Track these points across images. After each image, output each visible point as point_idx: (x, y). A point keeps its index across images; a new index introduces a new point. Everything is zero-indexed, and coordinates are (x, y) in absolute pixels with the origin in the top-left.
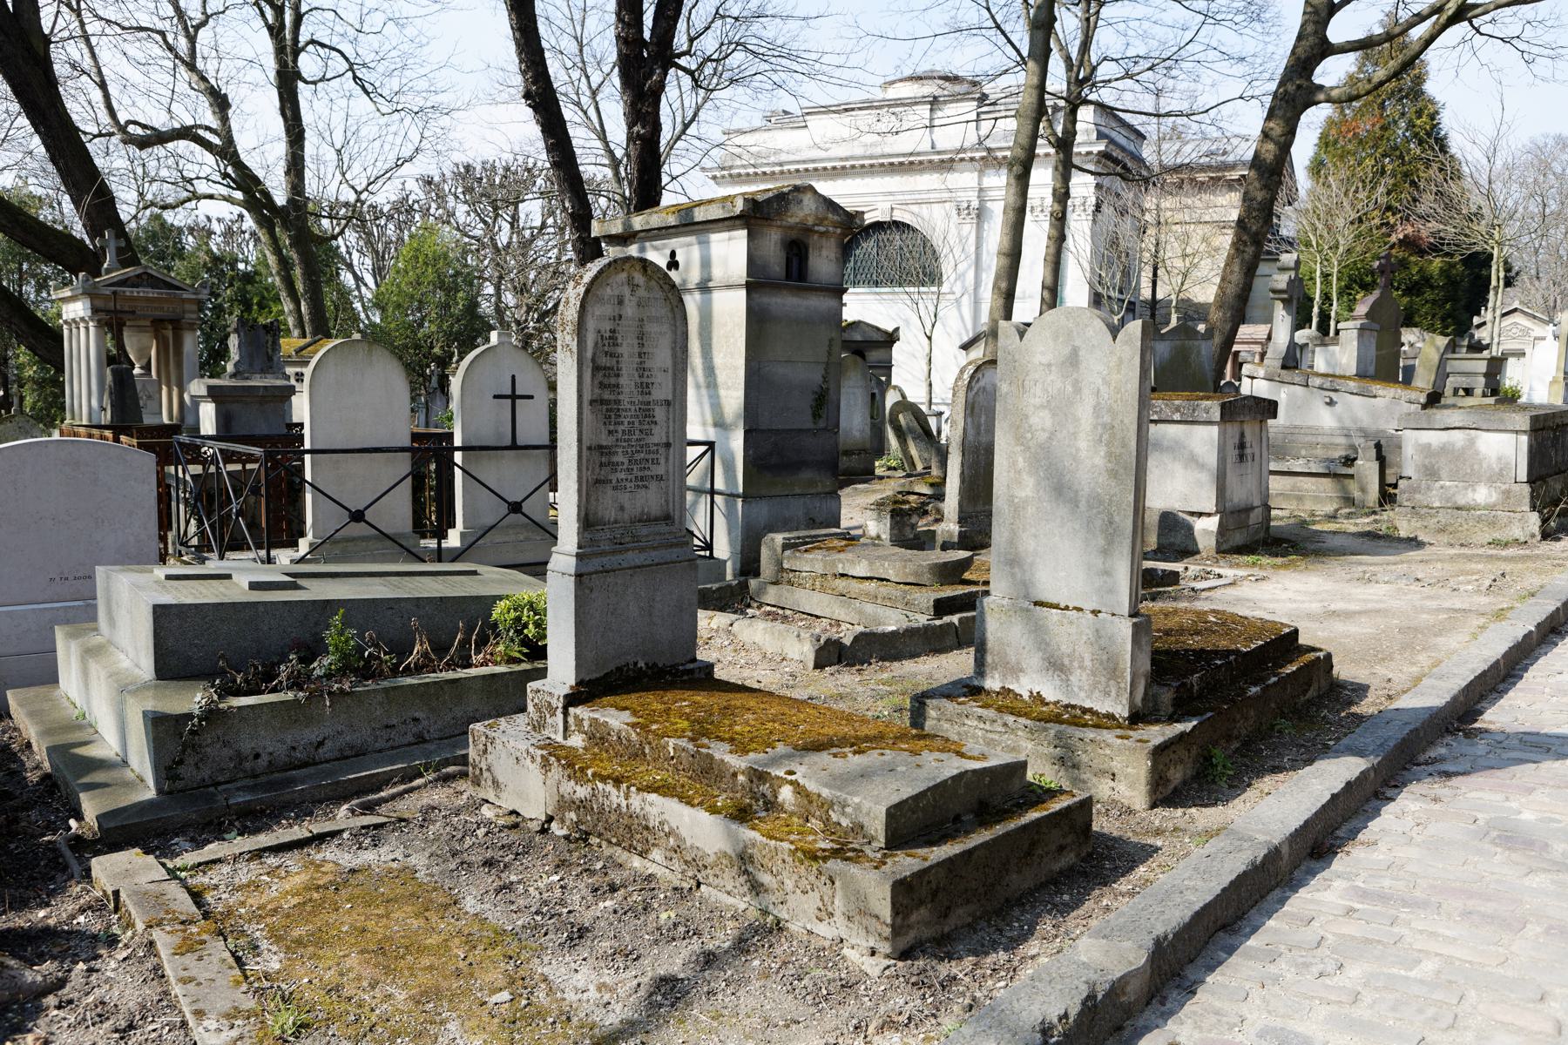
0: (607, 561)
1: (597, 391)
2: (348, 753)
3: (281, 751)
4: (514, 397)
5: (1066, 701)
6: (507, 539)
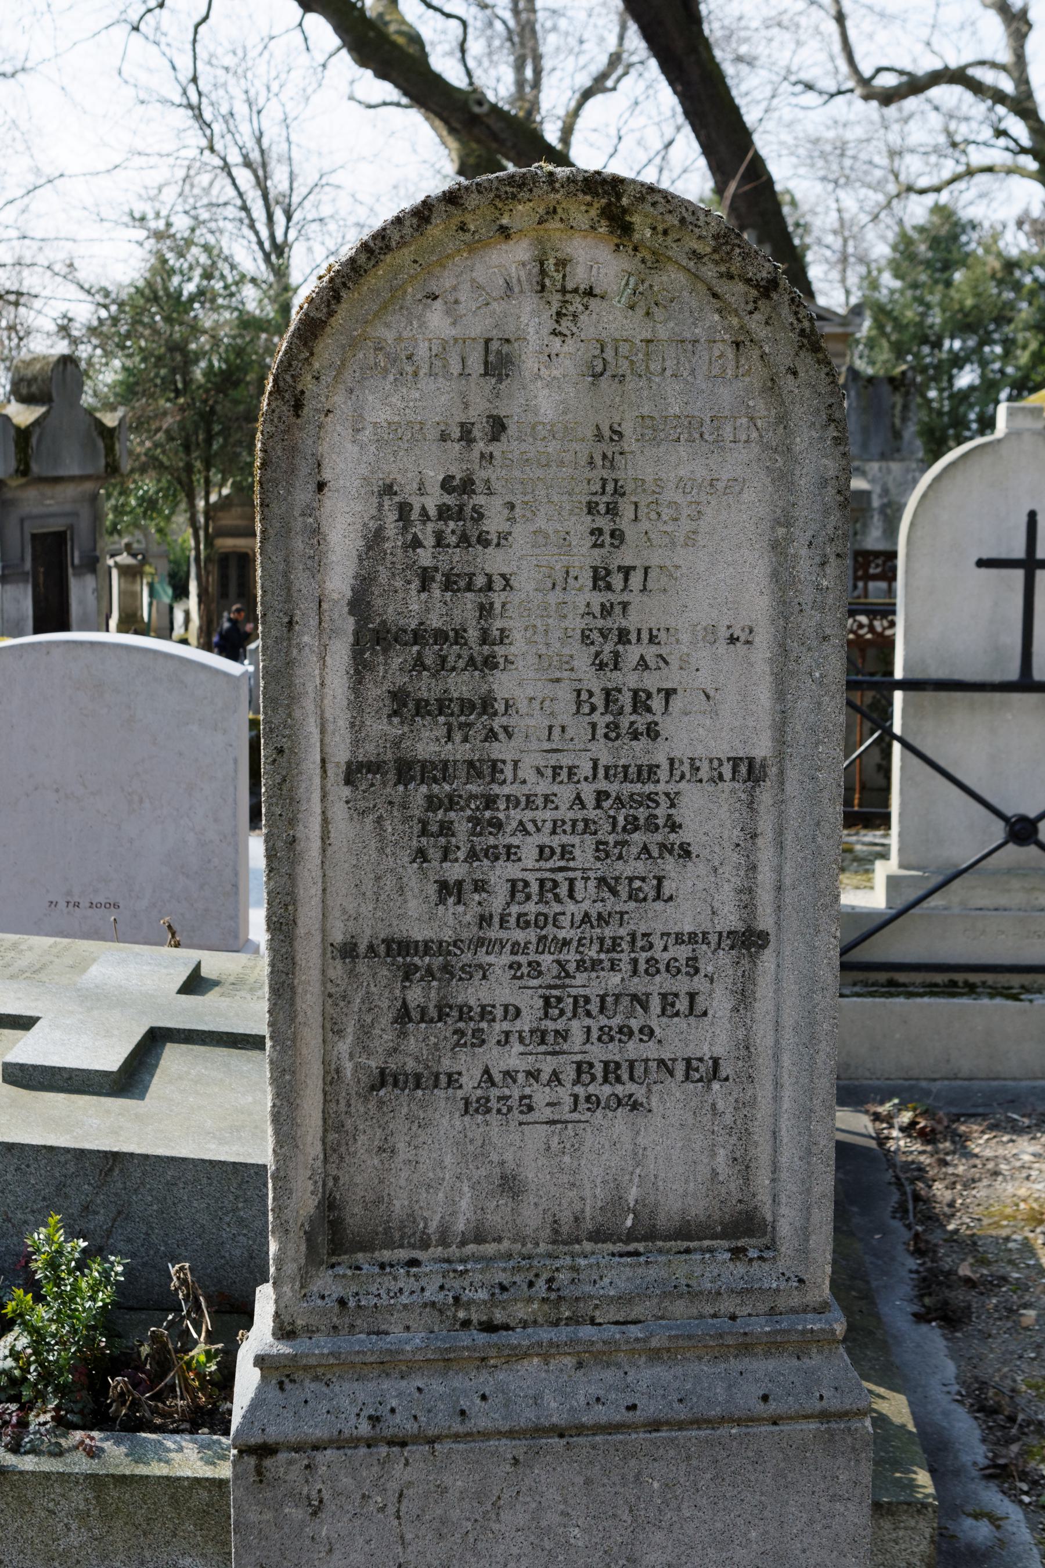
6: (1003, 901)
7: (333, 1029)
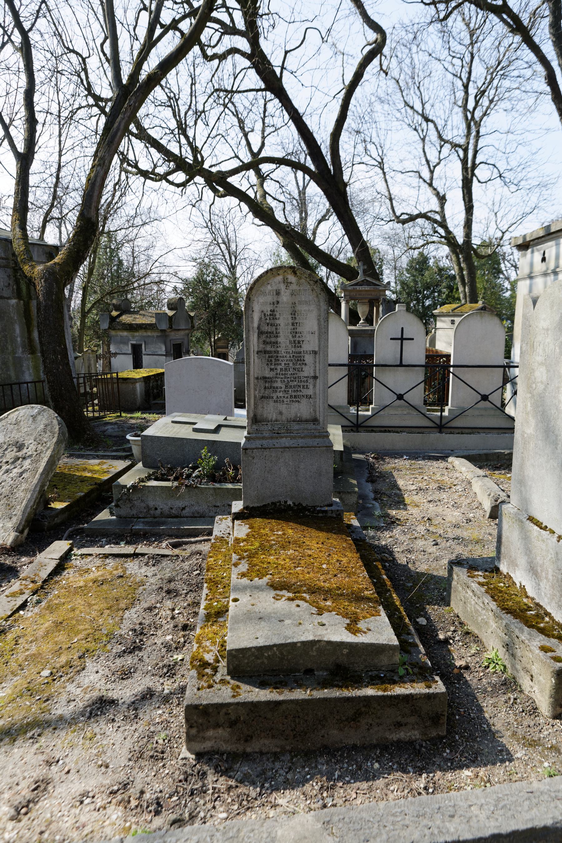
0: (265, 443)
1: (262, 346)
2: (196, 515)
3: (166, 508)
4: (402, 339)
5: (537, 601)
6: (397, 413)
7: (255, 390)
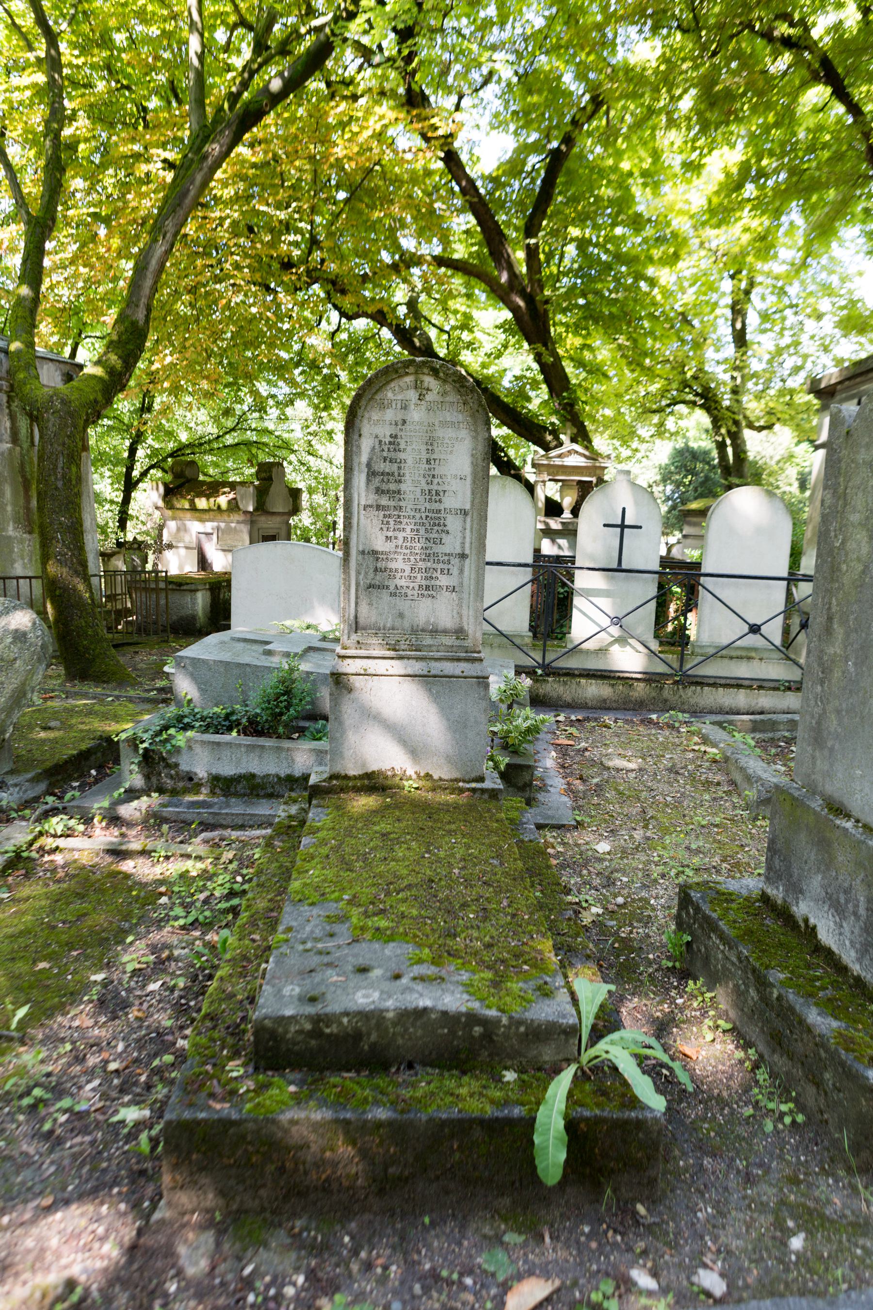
7: (358, 573)
